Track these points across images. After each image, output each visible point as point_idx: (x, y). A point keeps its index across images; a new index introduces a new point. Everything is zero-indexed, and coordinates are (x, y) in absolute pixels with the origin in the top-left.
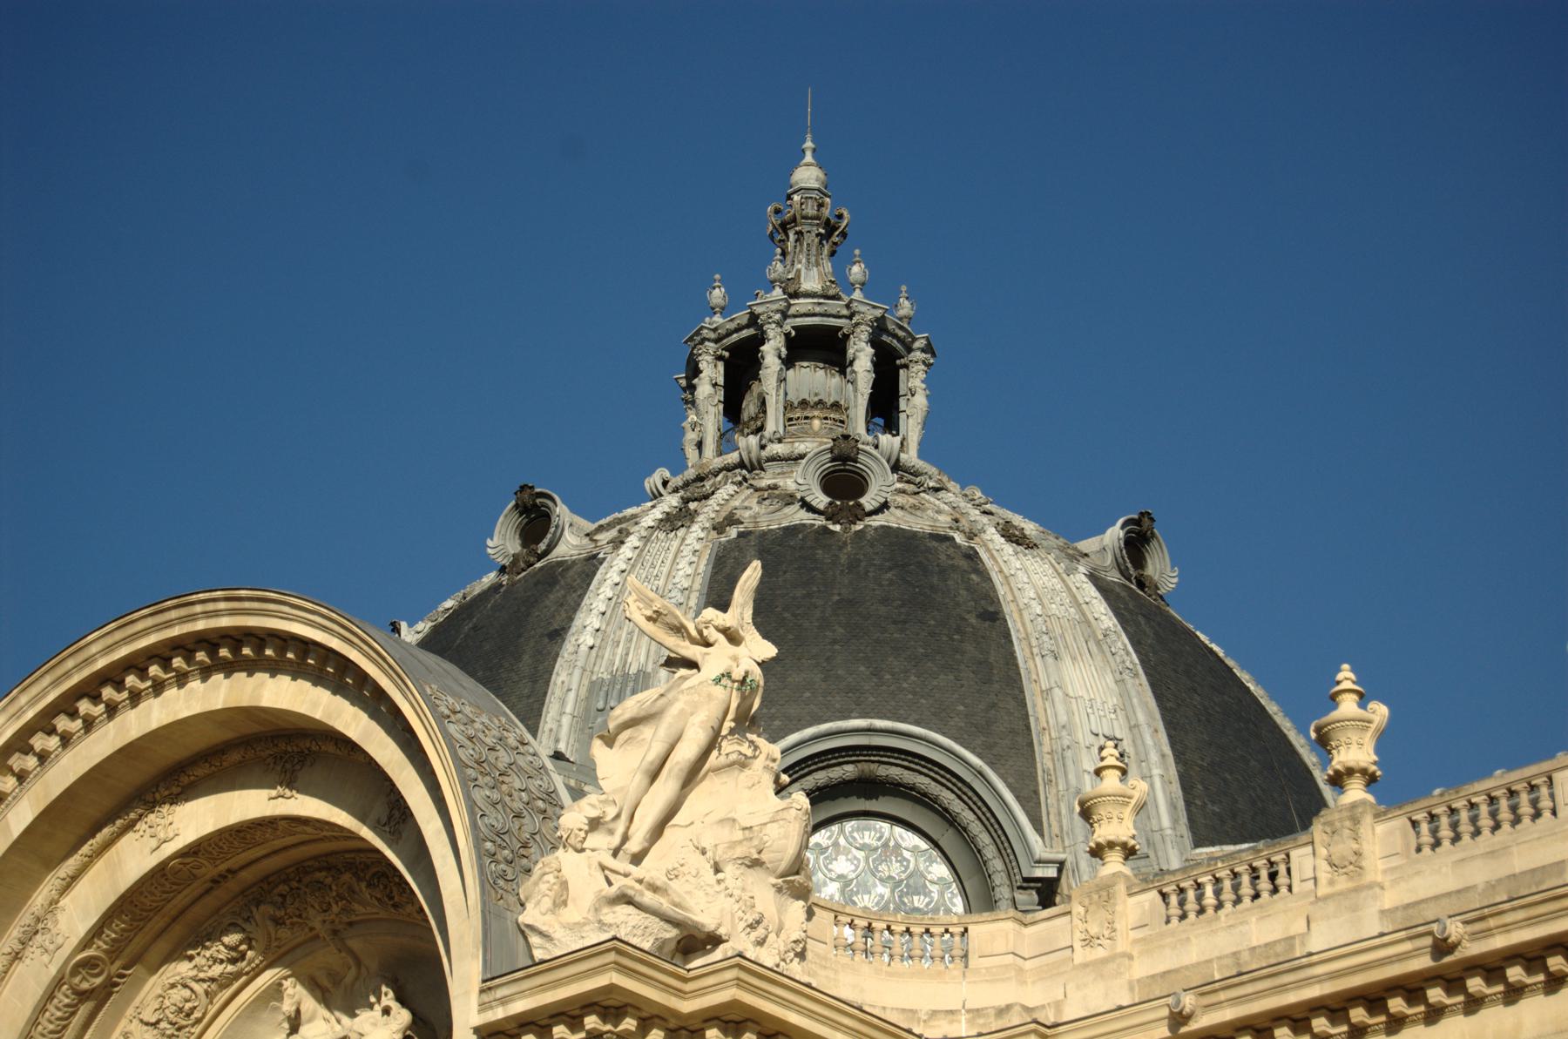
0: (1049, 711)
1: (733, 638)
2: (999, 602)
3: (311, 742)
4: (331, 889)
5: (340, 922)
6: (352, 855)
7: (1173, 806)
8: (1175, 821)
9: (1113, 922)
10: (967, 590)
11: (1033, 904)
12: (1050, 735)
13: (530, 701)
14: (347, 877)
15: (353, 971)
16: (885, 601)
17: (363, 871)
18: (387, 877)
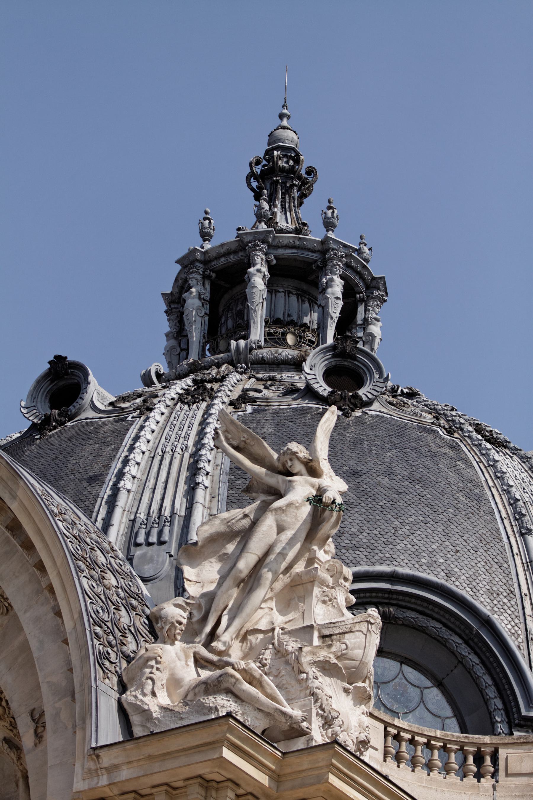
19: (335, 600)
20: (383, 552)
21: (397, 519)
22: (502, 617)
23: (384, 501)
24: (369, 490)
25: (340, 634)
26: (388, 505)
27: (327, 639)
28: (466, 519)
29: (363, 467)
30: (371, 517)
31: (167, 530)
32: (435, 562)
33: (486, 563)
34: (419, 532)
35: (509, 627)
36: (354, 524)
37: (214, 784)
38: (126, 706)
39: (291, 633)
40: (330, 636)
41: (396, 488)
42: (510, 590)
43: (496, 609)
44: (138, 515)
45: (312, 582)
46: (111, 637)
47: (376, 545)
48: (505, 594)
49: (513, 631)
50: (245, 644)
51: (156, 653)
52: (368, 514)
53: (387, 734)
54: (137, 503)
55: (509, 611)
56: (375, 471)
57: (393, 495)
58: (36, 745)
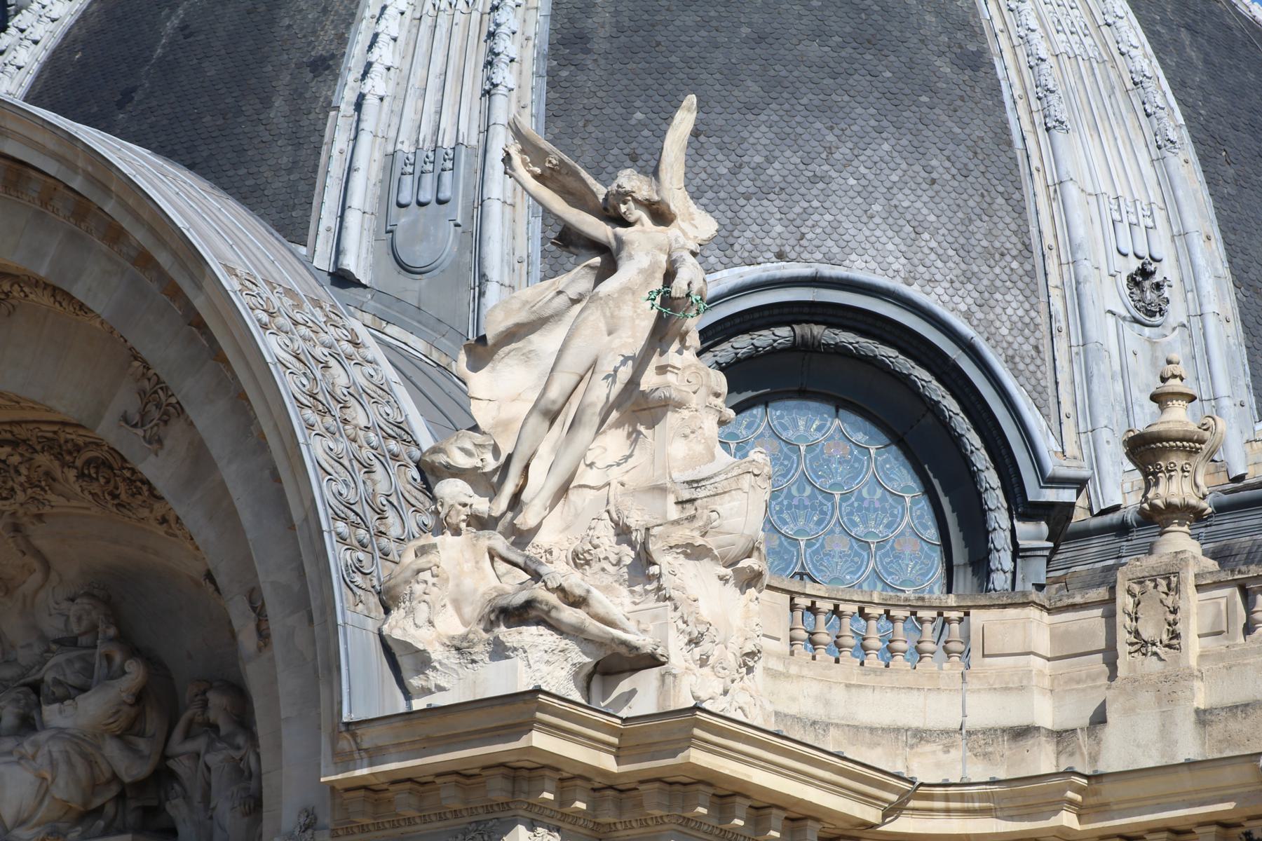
1: (660, 215)
2: (983, 34)
3: (12, 286)
4: (18, 473)
5: (25, 514)
6: (55, 428)
7: (1230, 358)
8: (1233, 382)
9: (1175, 623)
10: (938, 14)
11: (1040, 539)
12: (1059, 256)
13: (292, 177)
14: (43, 459)
15: (37, 577)
16: (820, 34)
17: (70, 453)
18: (111, 468)
19: (700, 431)
20: (807, 198)
21: (831, 128)
22: (1008, 297)
23: (810, 96)
24: (784, 73)
26: (816, 102)
27: (688, 506)
28: (951, 113)
29: (775, 25)
30: (788, 130)
31: (447, 176)
32: (896, 206)
33: (982, 195)
34: (869, 152)
35: (1020, 312)
36: (759, 147)
37: (525, 773)
38: (390, 643)
39: (634, 492)
40: (692, 501)
41: (832, 64)
42: (1024, 243)
43: (998, 283)
44: (399, 146)
45: (665, 406)
46: (362, 532)
47: (796, 185)
48: (1014, 252)
49: (1027, 320)
50: (566, 508)
52: (782, 124)
53: (793, 607)
54: (395, 120)
55: (1020, 284)
56: (795, 32)
57: (825, 82)
58: (260, 649)
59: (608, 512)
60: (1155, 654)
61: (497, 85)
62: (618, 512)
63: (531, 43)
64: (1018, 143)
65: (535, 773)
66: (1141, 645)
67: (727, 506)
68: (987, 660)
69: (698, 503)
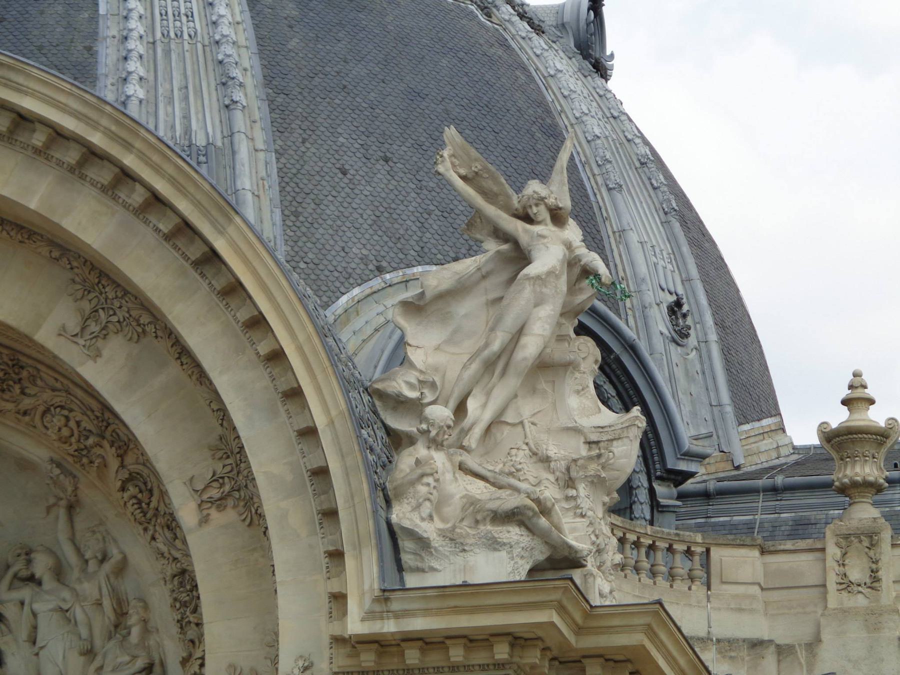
0: (624, 257)
9: (877, 571)
11: (671, 498)
25: (608, 440)
27: (594, 446)
38: (396, 529)
40: (597, 443)
51: (433, 469)
59: (527, 444)
60: (860, 592)
61: (237, 102)
62: (536, 444)
63: (249, 73)
64: (592, 198)
65: (529, 643)
66: (846, 585)
67: (620, 449)
68: (725, 587)
69: (602, 444)
